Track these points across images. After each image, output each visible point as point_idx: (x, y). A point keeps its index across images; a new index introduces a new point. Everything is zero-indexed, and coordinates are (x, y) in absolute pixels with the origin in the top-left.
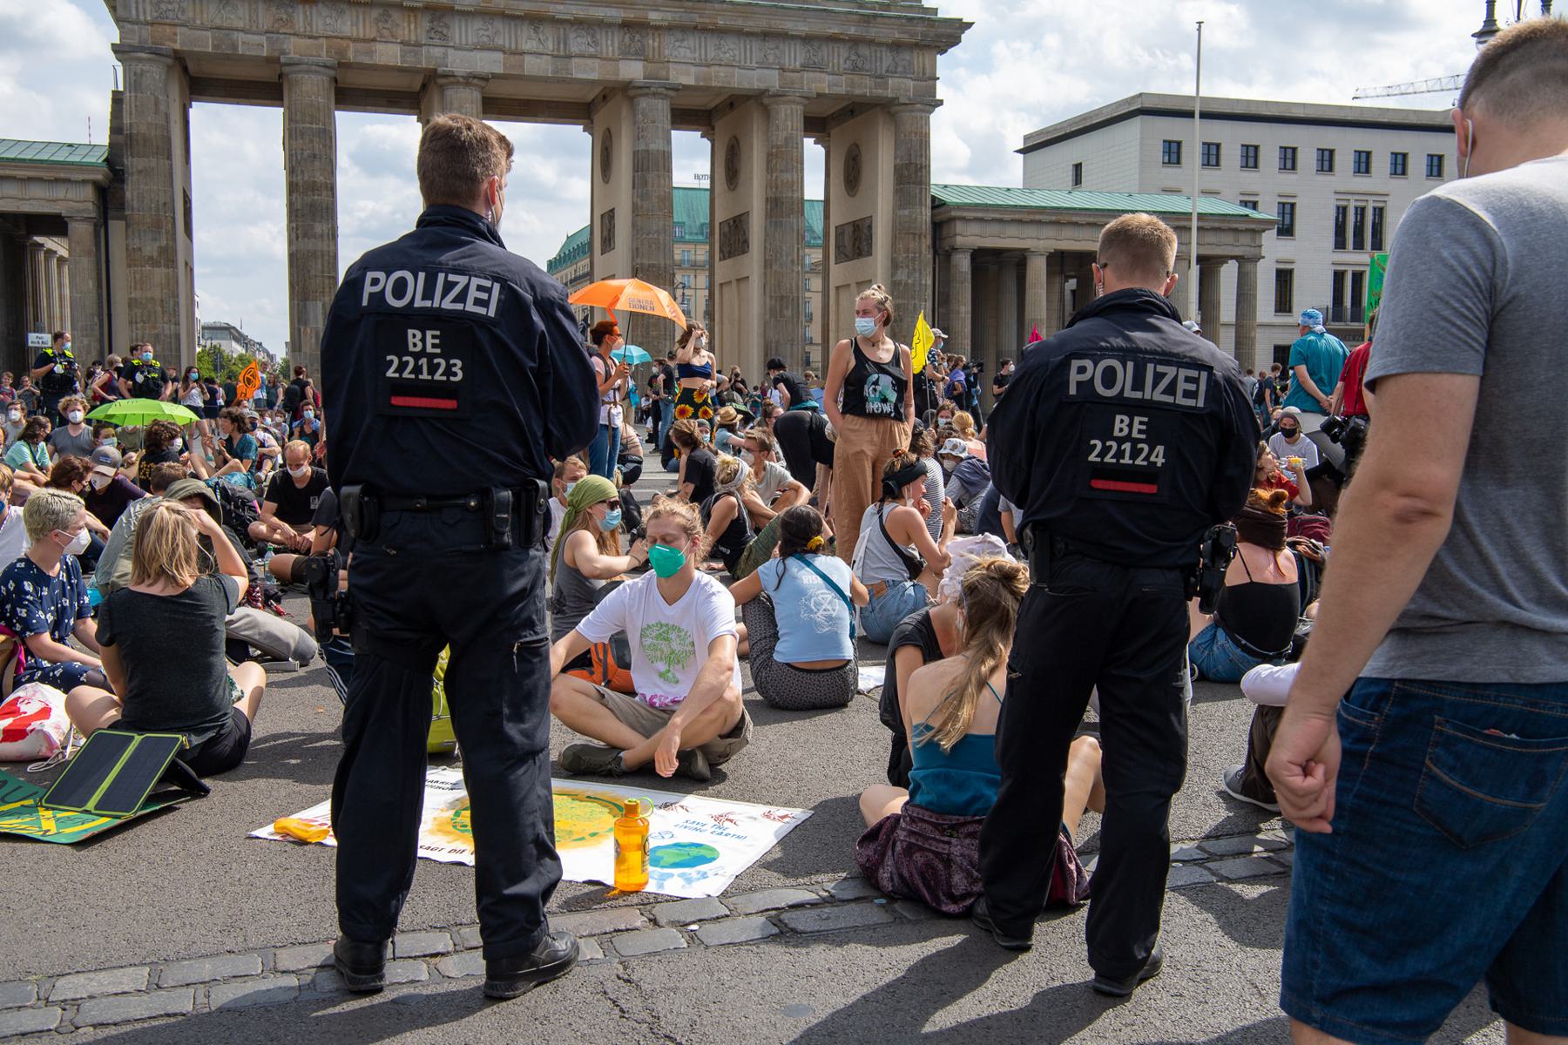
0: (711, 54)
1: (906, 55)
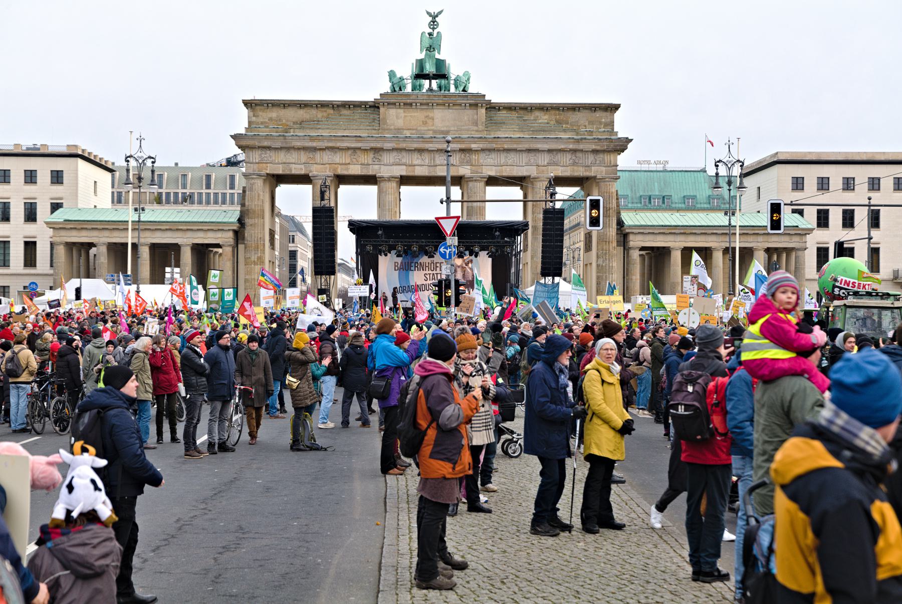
1: (601, 156)
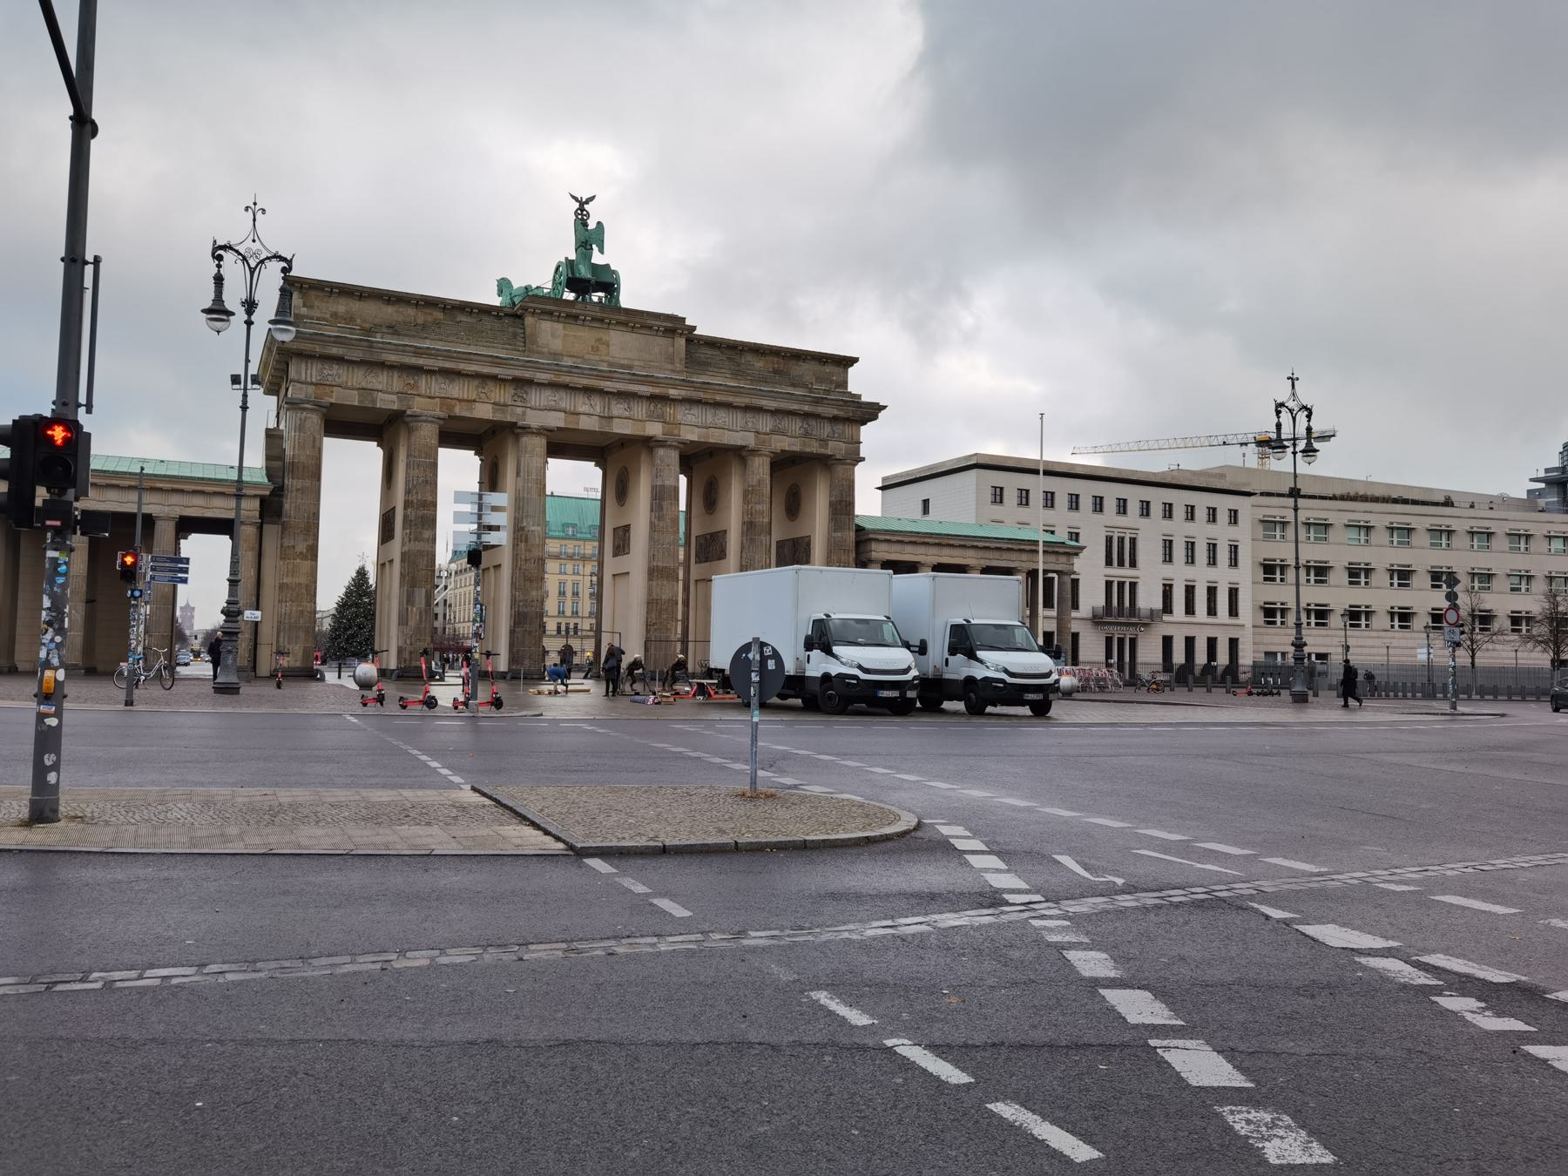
0: (710, 419)
1: (839, 428)
